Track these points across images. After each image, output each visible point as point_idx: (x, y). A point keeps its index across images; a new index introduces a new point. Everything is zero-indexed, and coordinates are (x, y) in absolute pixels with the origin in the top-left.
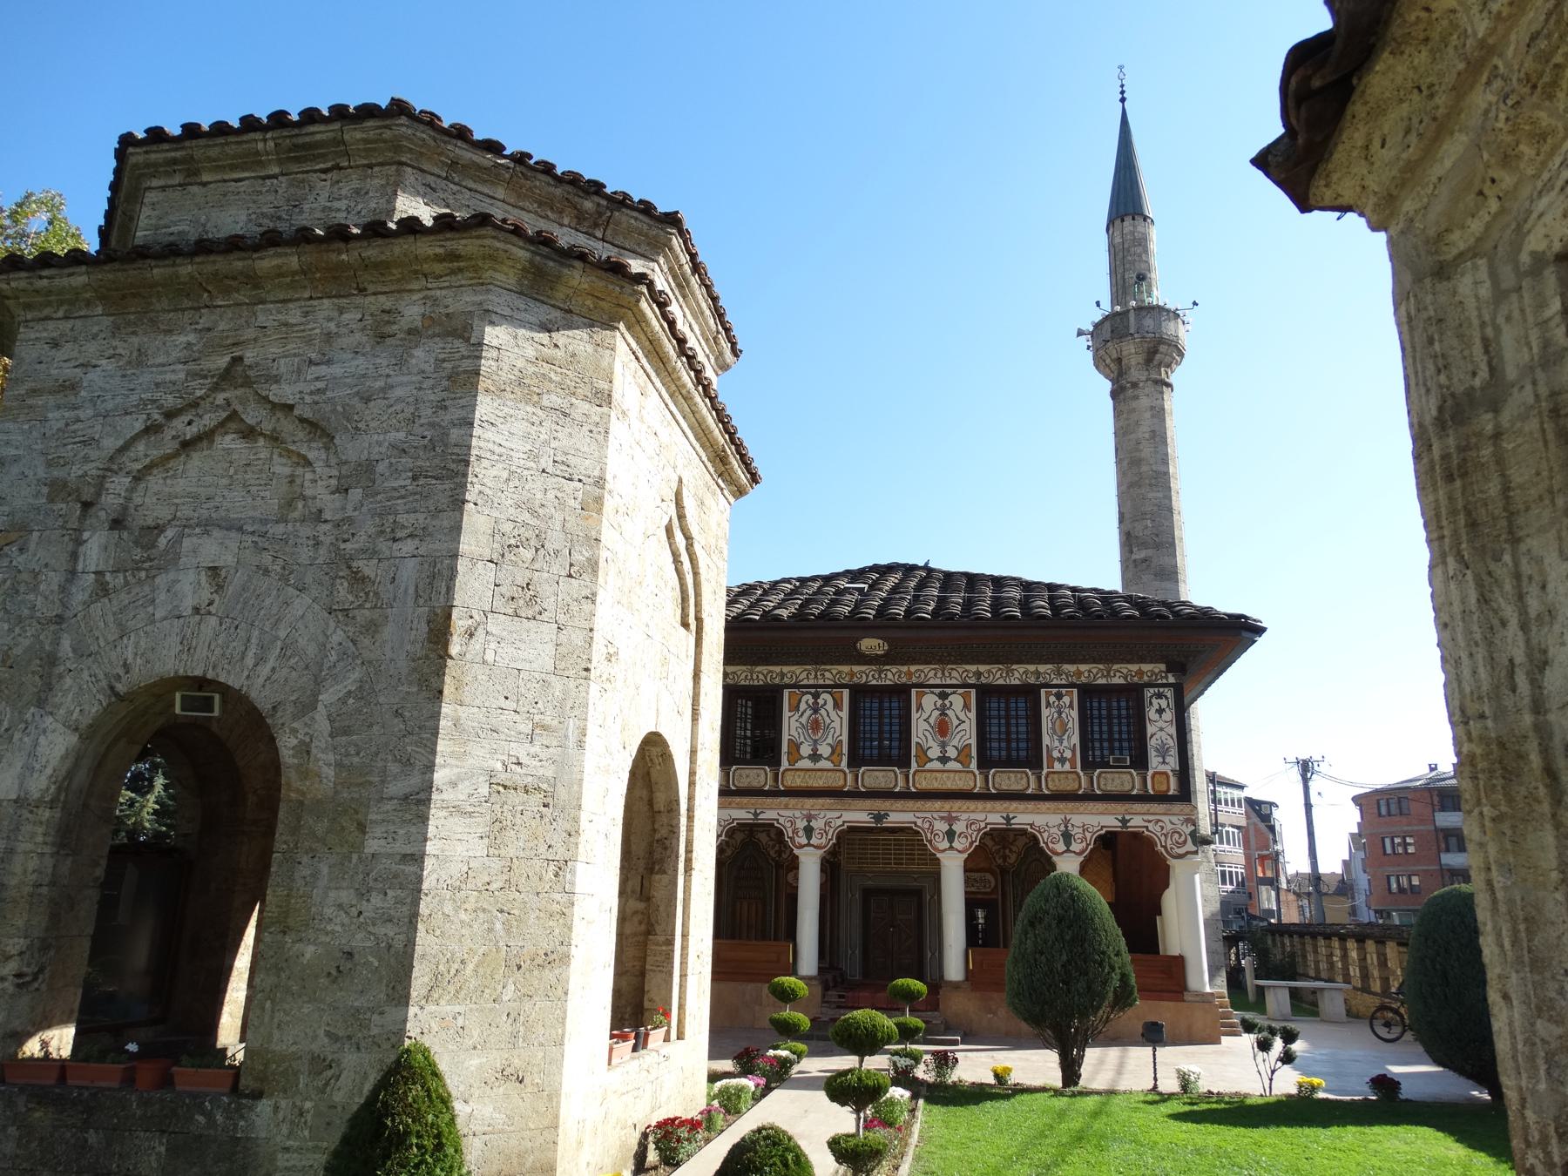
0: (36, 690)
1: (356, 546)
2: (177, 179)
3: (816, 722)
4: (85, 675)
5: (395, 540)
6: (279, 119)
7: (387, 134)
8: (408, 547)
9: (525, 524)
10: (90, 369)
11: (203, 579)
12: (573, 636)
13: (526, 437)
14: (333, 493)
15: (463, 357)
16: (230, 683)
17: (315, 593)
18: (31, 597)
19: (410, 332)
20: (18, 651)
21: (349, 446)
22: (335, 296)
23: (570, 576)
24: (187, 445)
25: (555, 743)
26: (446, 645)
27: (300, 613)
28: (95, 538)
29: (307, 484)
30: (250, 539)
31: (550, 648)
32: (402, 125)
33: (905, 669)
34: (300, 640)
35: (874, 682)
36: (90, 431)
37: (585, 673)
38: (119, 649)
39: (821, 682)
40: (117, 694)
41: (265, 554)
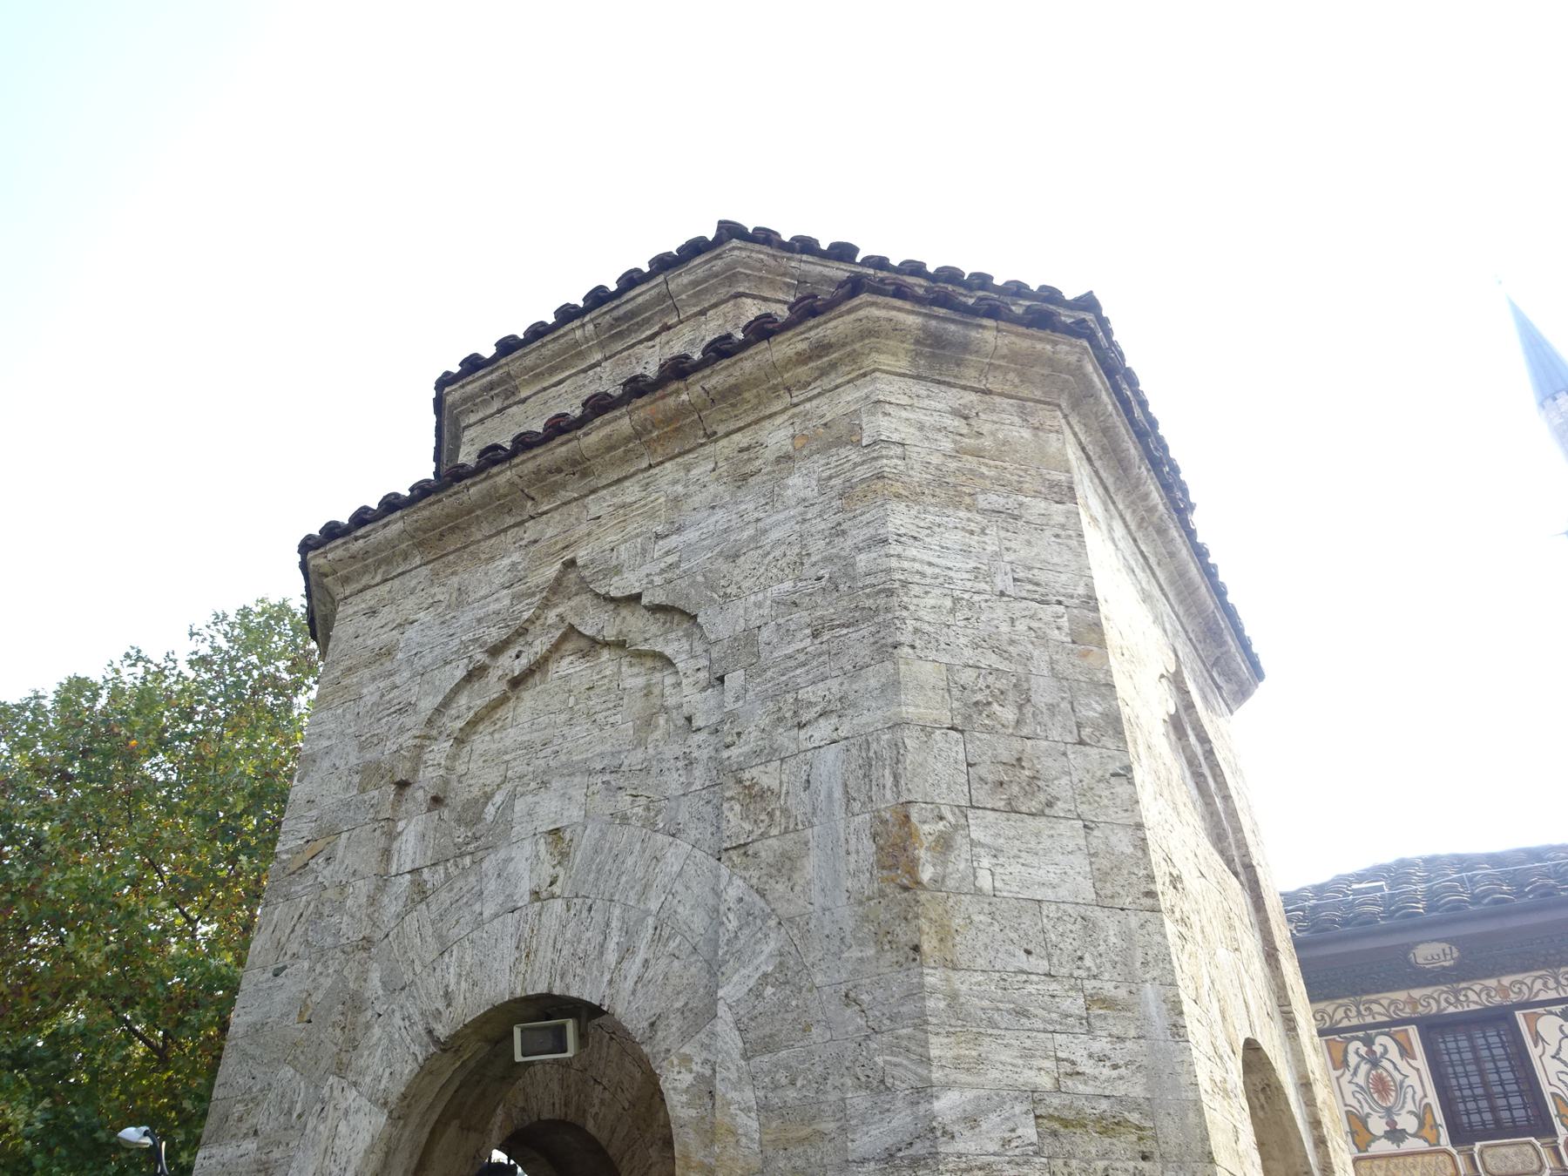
0: (335, 1050)
1: (746, 749)
2: (496, 405)
3: (1380, 1079)
4: (398, 1015)
5: (800, 726)
6: (598, 297)
7: (718, 265)
8: (823, 730)
9: (993, 671)
10: (407, 626)
11: (542, 848)
12: (1113, 840)
13: (966, 551)
14: (704, 689)
15: (856, 465)
16: (586, 998)
17: (693, 834)
18: (336, 919)
19: (778, 460)
20: (318, 997)
21: (718, 620)
22: (680, 454)
23: (1081, 742)
24: (516, 683)
25: (1132, 1033)
26: (912, 866)
27: (676, 868)
28: (411, 827)
29: (667, 692)
30: (599, 779)
31: (1080, 863)
32: (734, 248)
33: (1492, 983)
34: (681, 909)
35: (1451, 1009)
36: (405, 696)
37: (1148, 902)
38: (438, 970)
39: (1369, 1020)
40: (436, 1041)
41: (621, 793)
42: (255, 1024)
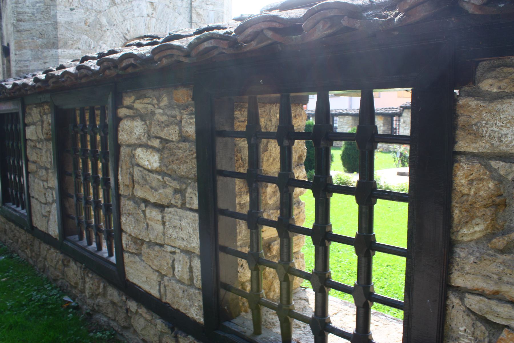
4: (114, 32)
5: (207, 4)
8: (211, 7)
38: (124, 24)
42: (68, 22)
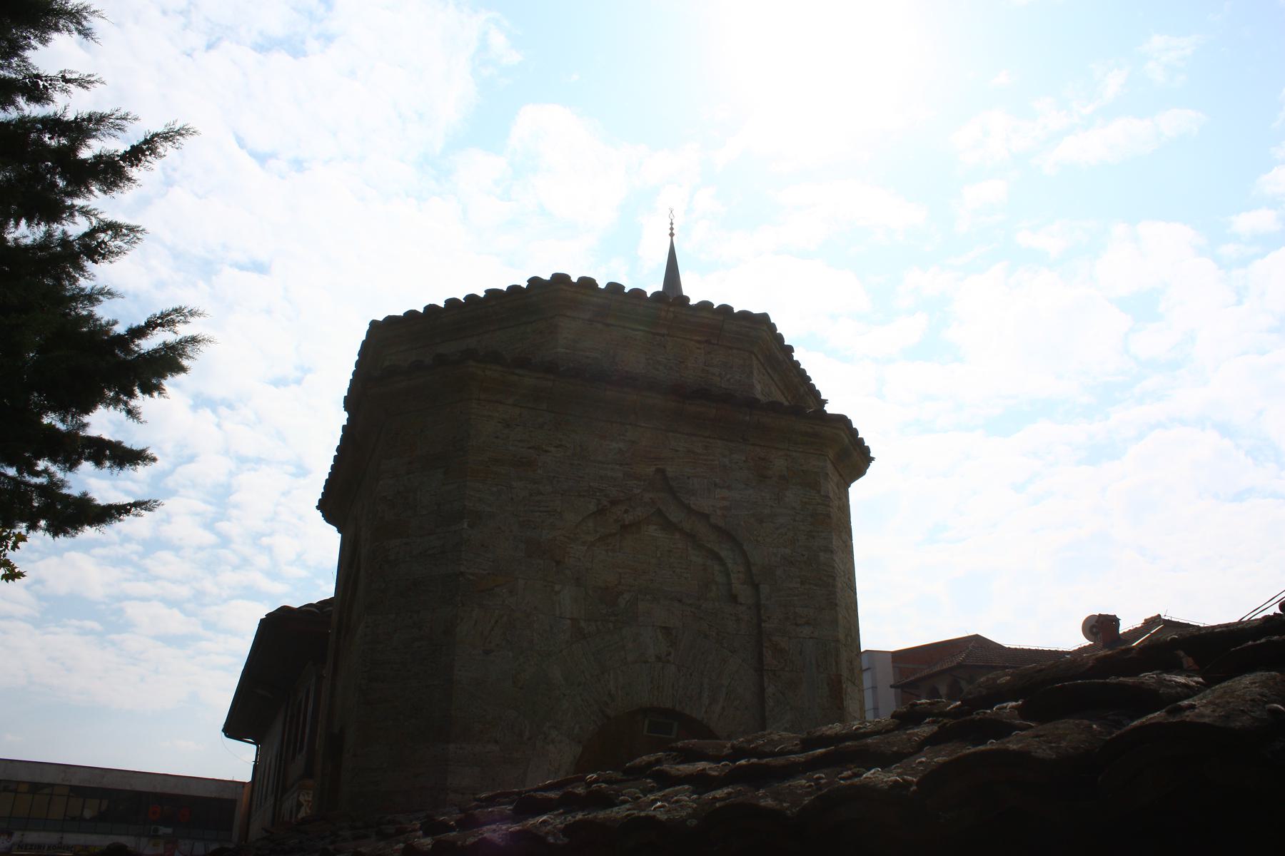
5: (796, 625)
15: (818, 504)
24: (625, 528)
